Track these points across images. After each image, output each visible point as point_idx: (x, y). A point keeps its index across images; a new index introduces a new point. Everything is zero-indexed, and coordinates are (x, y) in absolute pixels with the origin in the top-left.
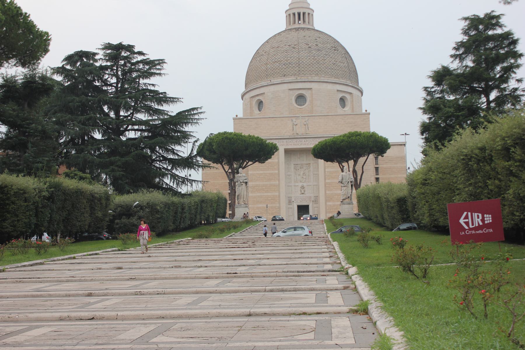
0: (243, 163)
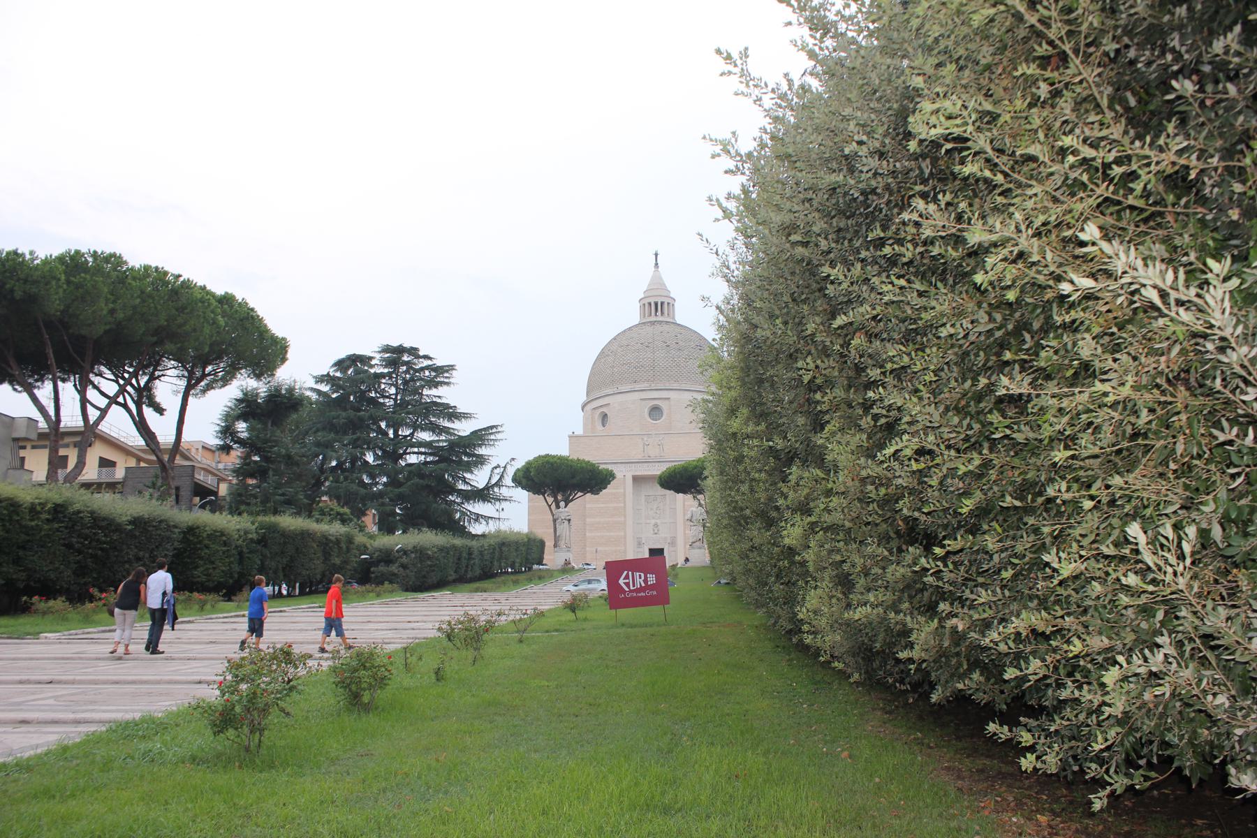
0: (570, 495)
